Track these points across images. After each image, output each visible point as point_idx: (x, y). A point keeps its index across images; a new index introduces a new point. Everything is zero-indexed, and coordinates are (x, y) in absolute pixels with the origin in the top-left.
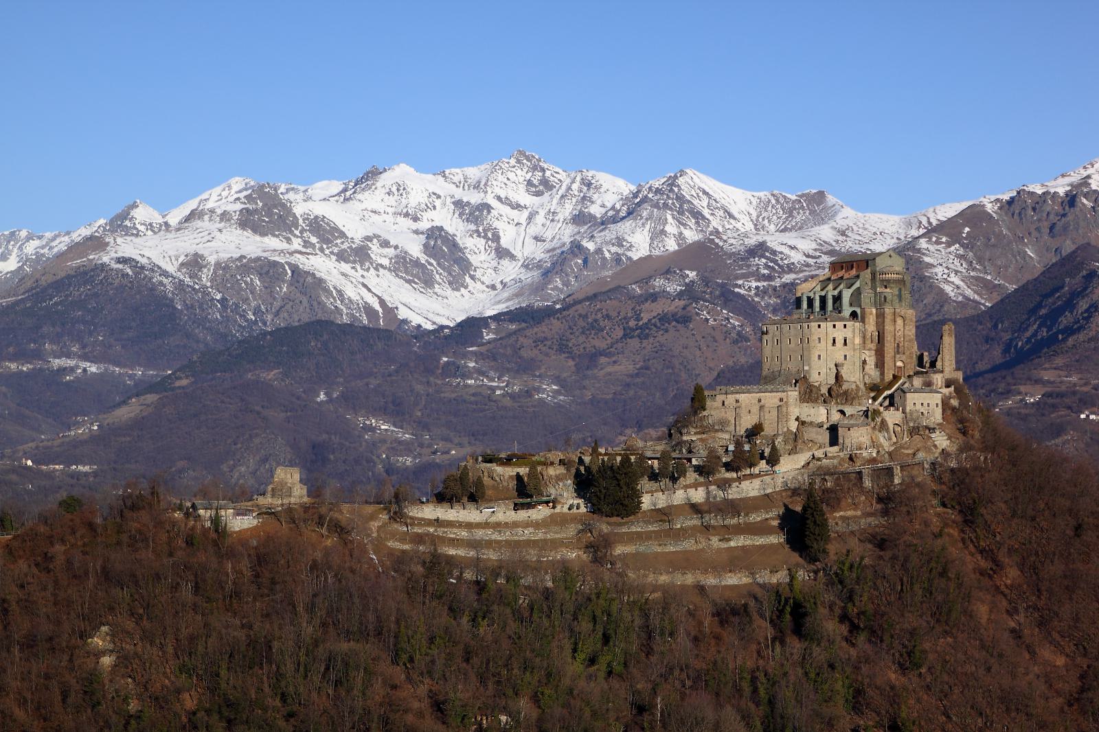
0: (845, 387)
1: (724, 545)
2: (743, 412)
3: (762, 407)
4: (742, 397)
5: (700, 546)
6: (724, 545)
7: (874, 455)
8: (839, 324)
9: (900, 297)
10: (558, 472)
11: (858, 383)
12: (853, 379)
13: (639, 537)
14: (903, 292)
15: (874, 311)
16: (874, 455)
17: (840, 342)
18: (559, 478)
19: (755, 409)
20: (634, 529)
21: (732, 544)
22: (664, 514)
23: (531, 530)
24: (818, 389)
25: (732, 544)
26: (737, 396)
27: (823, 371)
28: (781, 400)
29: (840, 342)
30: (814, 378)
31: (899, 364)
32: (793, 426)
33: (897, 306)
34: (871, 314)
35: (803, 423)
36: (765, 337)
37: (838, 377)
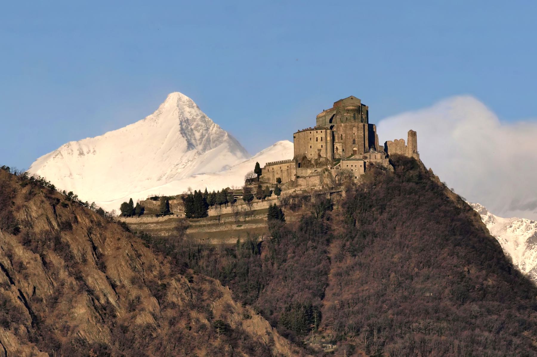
0: (321, 159)
1: (239, 228)
2: (275, 174)
3: (282, 171)
4: (275, 167)
5: (226, 229)
6: (239, 228)
7: (321, 188)
8: (319, 131)
9: (354, 118)
10: (178, 202)
11: (329, 158)
12: (325, 156)
13: (200, 226)
14: (356, 115)
15: (343, 125)
16: (321, 188)
17: (319, 139)
18: (178, 204)
19: (279, 172)
20: (202, 223)
21: (242, 228)
22: (218, 218)
23: (155, 225)
24: (310, 161)
25: (242, 228)
26: (273, 166)
27: (313, 153)
28: (288, 167)
29: (319, 139)
30: (309, 157)
31: (355, 149)
32: (293, 178)
33: (353, 121)
34: (341, 126)
35: (298, 177)
36: (295, 139)
37: (320, 156)
